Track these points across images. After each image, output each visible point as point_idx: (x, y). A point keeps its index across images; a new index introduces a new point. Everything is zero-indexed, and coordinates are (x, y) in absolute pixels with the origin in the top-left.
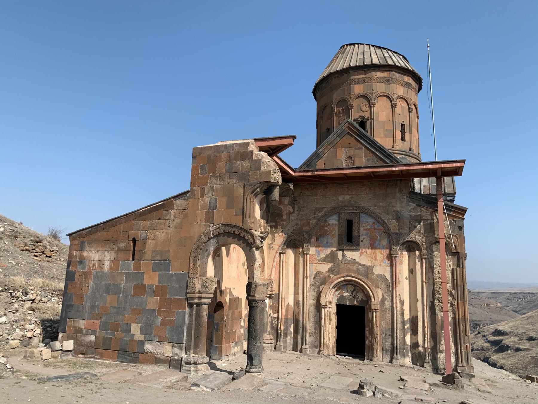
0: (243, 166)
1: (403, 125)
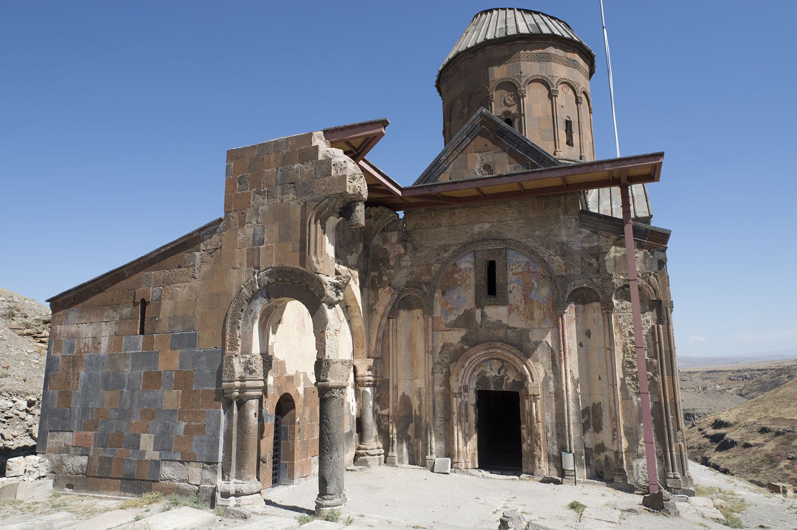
0: (302, 172)
1: (568, 124)
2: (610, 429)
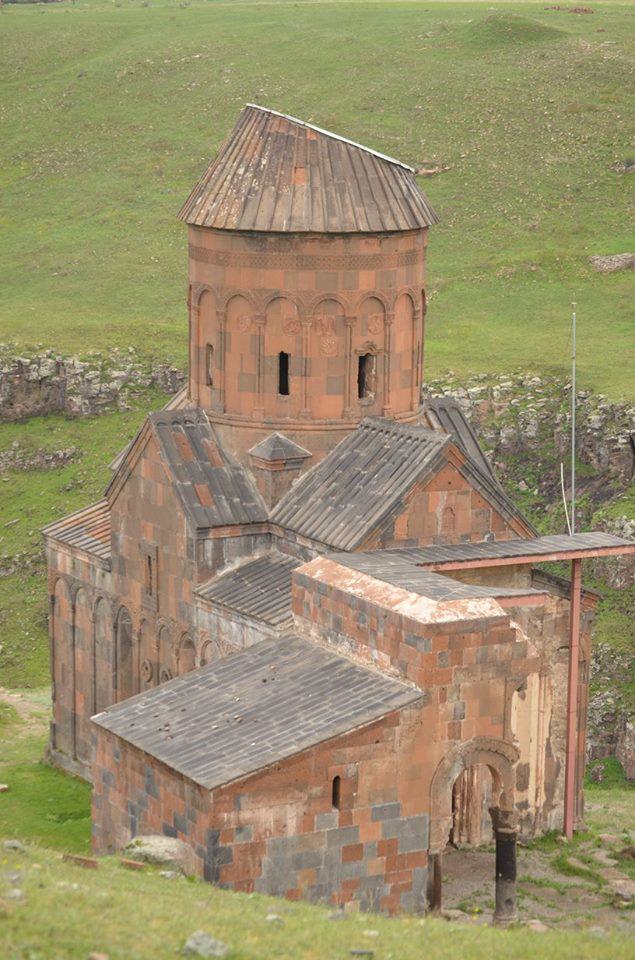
0: (501, 652)
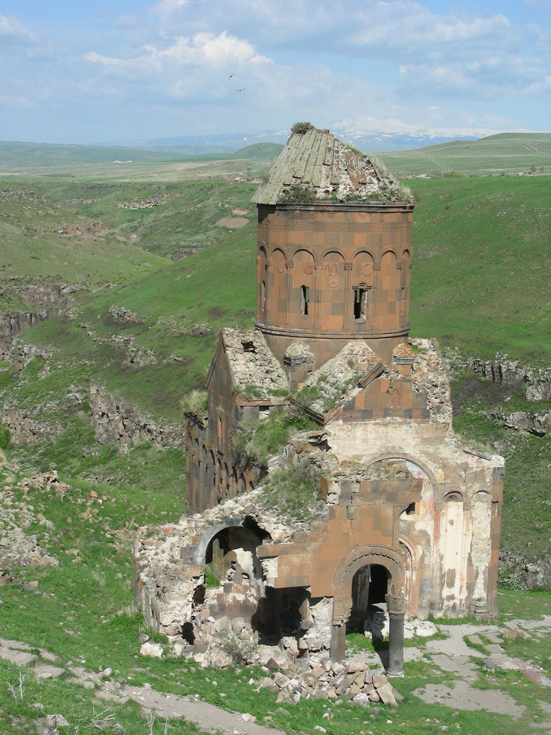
2: (459, 586)
